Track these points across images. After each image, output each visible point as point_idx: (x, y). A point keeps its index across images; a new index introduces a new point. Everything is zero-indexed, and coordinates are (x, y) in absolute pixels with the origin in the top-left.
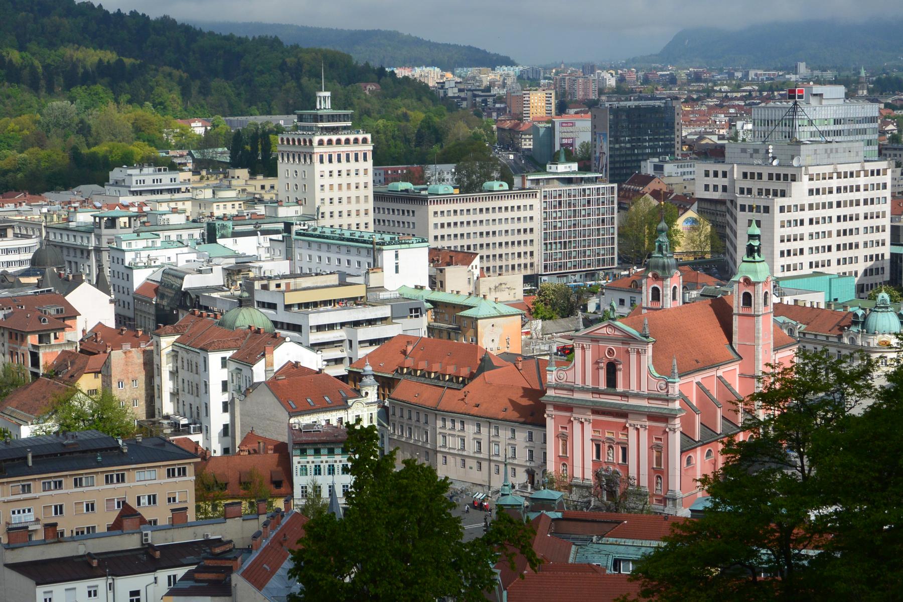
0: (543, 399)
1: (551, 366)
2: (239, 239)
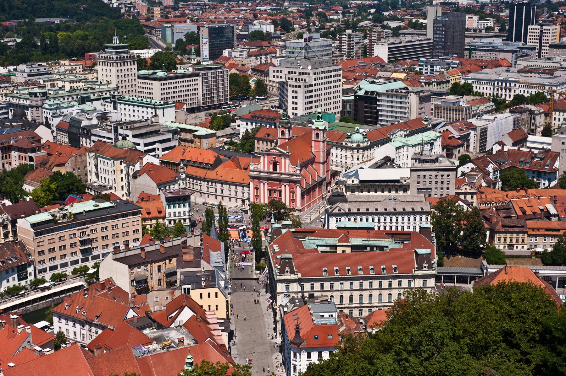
2: (94, 102)
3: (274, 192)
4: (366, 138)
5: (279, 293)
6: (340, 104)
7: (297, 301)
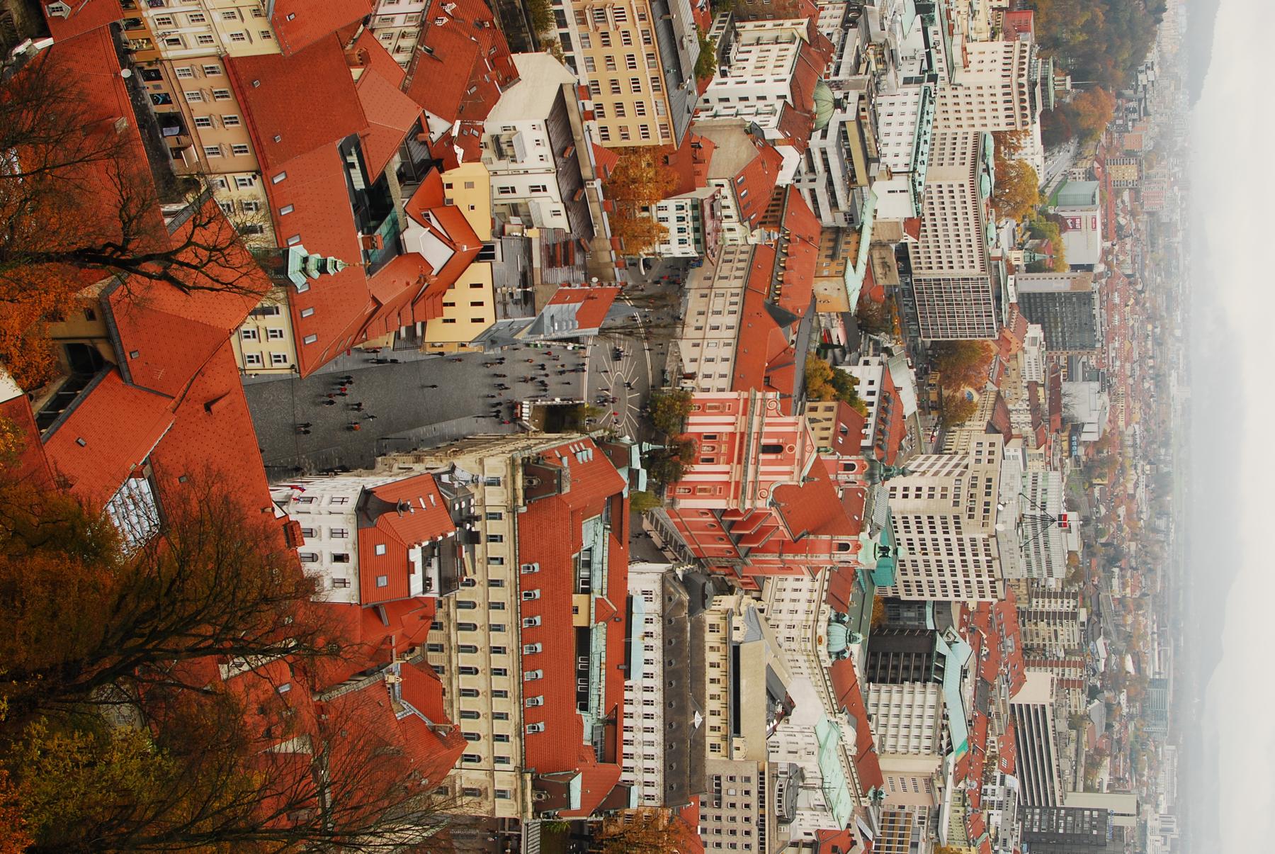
3: (714, 448)
4: (838, 658)
5: (481, 461)
6: (915, 597)
7: (464, 505)
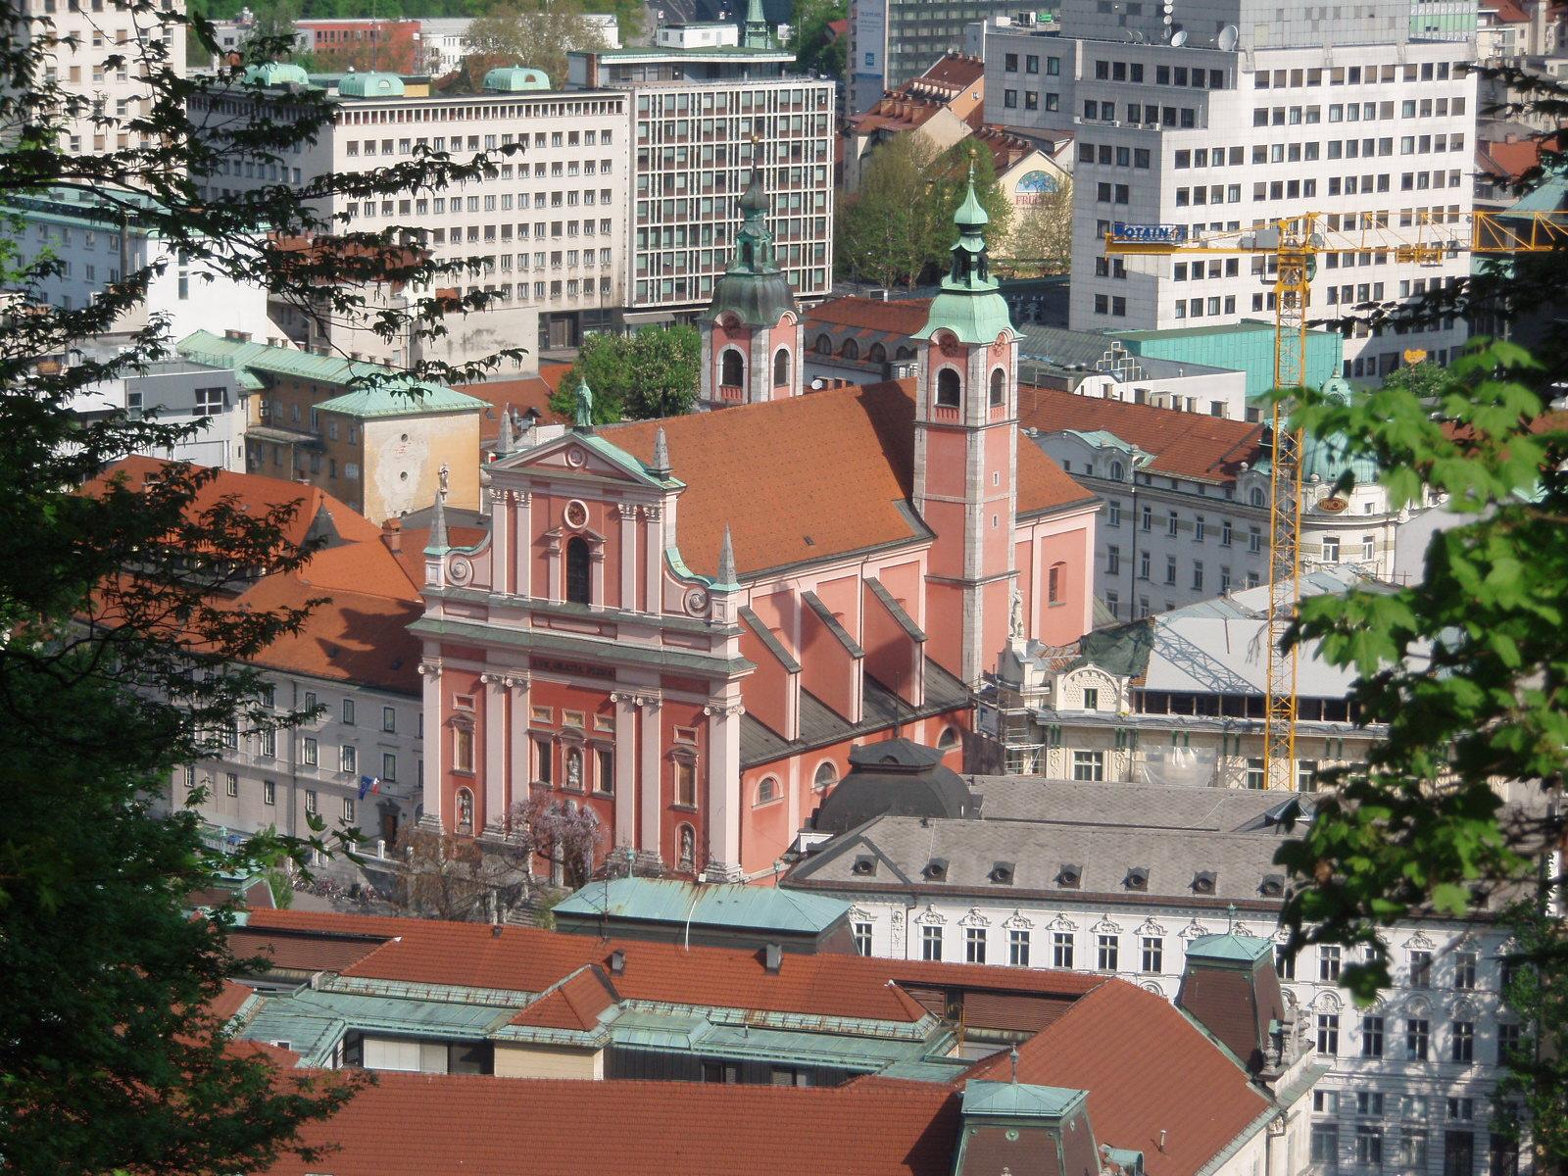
0: (415, 626)
1: (436, 545)
